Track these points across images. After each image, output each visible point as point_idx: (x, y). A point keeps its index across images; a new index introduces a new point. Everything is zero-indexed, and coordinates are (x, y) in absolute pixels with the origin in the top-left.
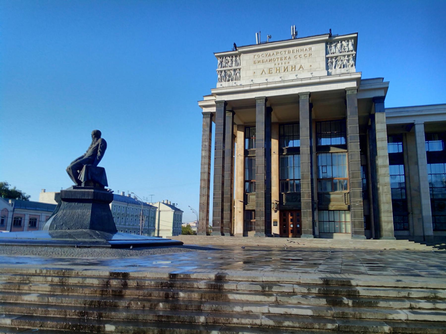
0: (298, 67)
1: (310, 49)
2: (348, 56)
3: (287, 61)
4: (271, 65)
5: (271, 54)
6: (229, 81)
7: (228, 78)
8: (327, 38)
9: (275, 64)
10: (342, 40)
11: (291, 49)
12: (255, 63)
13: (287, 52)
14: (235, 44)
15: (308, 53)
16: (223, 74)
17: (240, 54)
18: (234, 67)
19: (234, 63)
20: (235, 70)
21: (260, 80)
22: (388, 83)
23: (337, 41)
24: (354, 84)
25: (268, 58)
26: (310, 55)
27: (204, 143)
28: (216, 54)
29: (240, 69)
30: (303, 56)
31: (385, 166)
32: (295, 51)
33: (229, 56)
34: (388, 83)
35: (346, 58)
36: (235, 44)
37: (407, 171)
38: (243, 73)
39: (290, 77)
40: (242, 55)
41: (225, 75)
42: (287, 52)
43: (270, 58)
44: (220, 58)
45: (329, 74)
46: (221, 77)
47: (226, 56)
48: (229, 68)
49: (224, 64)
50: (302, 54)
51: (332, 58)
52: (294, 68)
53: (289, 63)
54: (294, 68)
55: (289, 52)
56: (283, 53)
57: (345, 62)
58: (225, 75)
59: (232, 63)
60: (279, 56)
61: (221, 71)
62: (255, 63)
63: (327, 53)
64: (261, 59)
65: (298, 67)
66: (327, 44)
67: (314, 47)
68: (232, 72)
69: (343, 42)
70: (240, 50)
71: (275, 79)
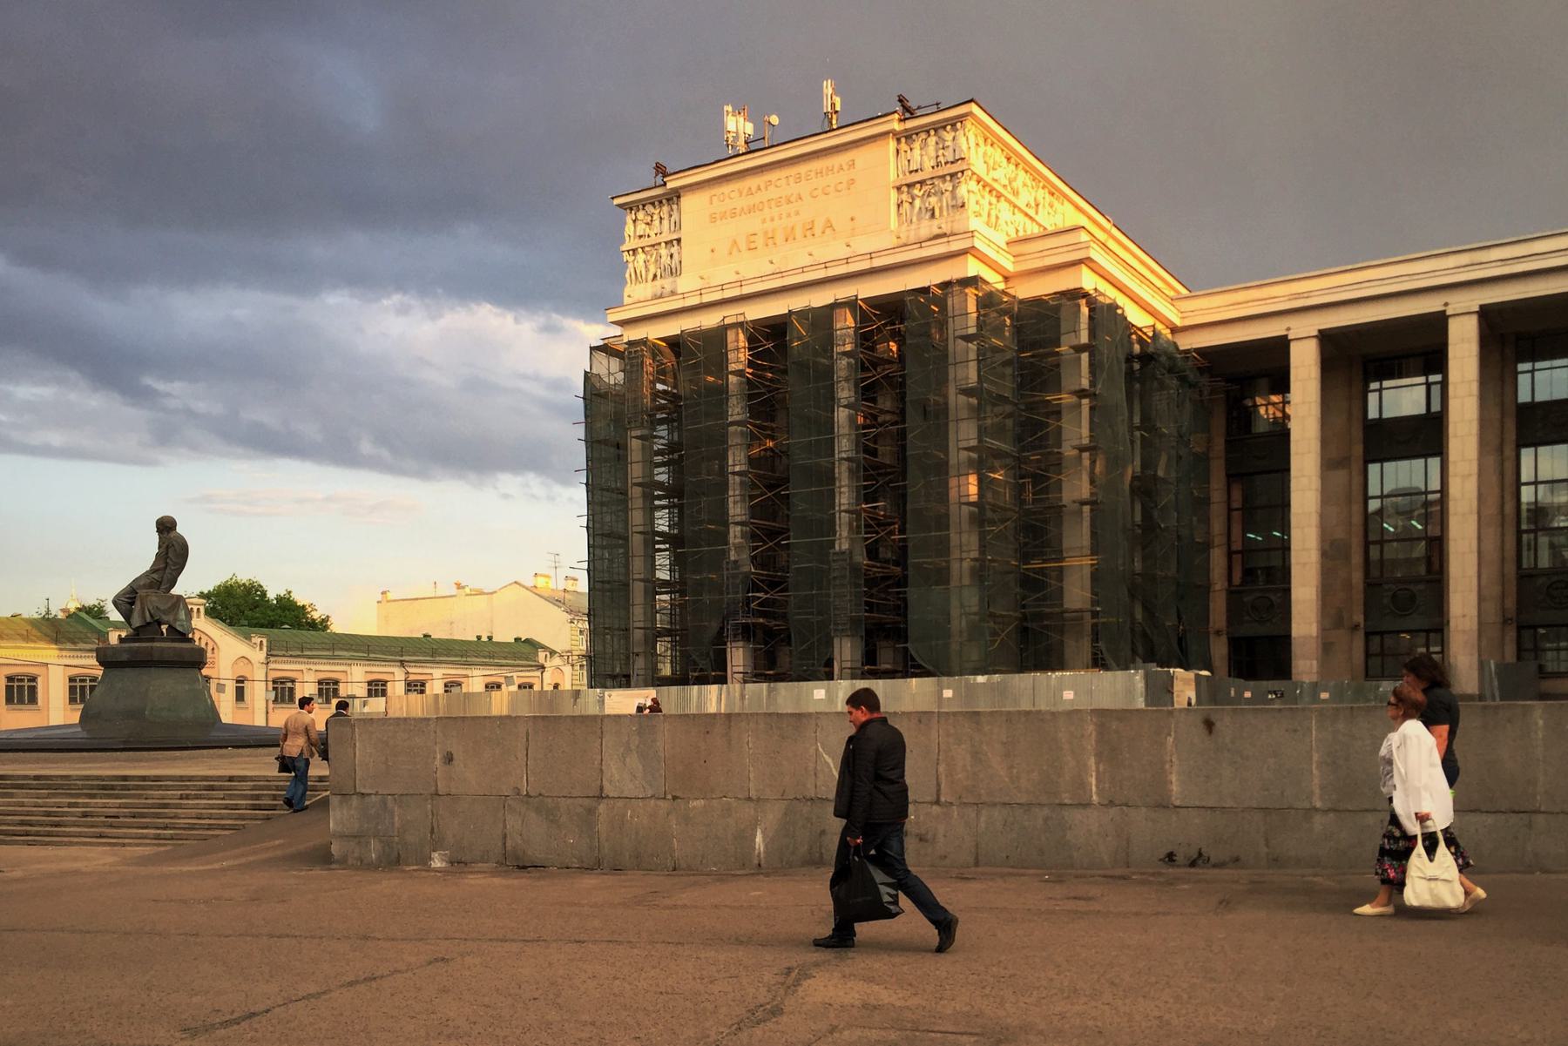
1: (852, 164)
9: (764, 221)
11: (802, 169)
12: (713, 219)
15: (844, 177)
18: (666, 237)
28: (616, 201)
29: (679, 240)
30: (831, 189)
37: (1509, 466)
38: (688, 253)
53: (797, 213)
56: (783, 182)
60: (773, 193)
62: (713, 219)
67: (861, 156)
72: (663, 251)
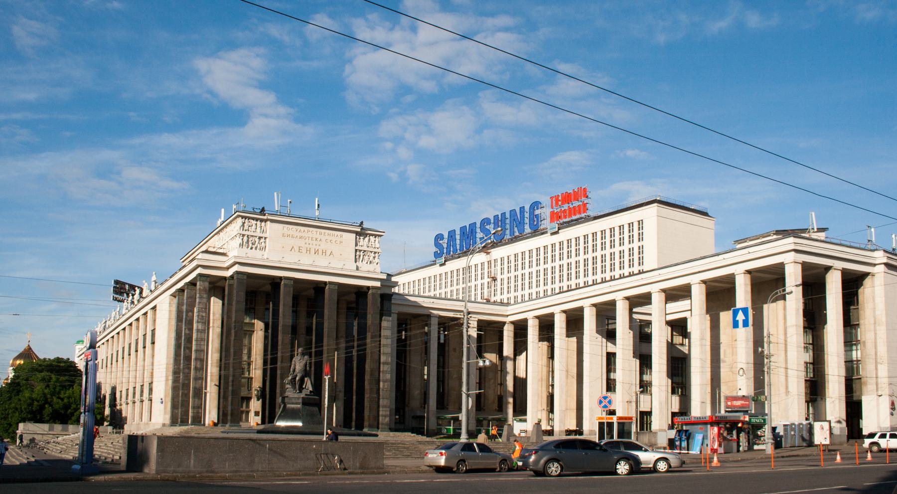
0: (328, 253)
1: (341, 236)
2: (375, 253)
3: (318, 243)
4: (301, 243)
7: (250, 245)
10: (372, 235)
15: (339, 239)
16: (245, 238)
17: (266, 221)
18: (258, 234)
19: (259, 229)
20: (260, 238)
23: (366, 235)
24: (378, 284)
25: (299, 234)
26: (341, 242)
31: (384, 363)
33: (253, 219)
35: (372, 255)
39: (322, 263)
40: (268, 223)
41: (248, 241)
43: (300, 234)
45: (357, 269)
47: (249, 218)
48: (252, 234)
49: (246, 227)
50: (334, 239)
51: (360, 251)
52: (324, 253)
54: (324, 253)
55: (321, 234)
57: (371, 258)
58: (248, 241)
60: (310, 234)
61: (243, 235)
63: (356, 245)
64: (290, 232)
65: (328, 253)
68: (257, 240)
71: (306, 261)
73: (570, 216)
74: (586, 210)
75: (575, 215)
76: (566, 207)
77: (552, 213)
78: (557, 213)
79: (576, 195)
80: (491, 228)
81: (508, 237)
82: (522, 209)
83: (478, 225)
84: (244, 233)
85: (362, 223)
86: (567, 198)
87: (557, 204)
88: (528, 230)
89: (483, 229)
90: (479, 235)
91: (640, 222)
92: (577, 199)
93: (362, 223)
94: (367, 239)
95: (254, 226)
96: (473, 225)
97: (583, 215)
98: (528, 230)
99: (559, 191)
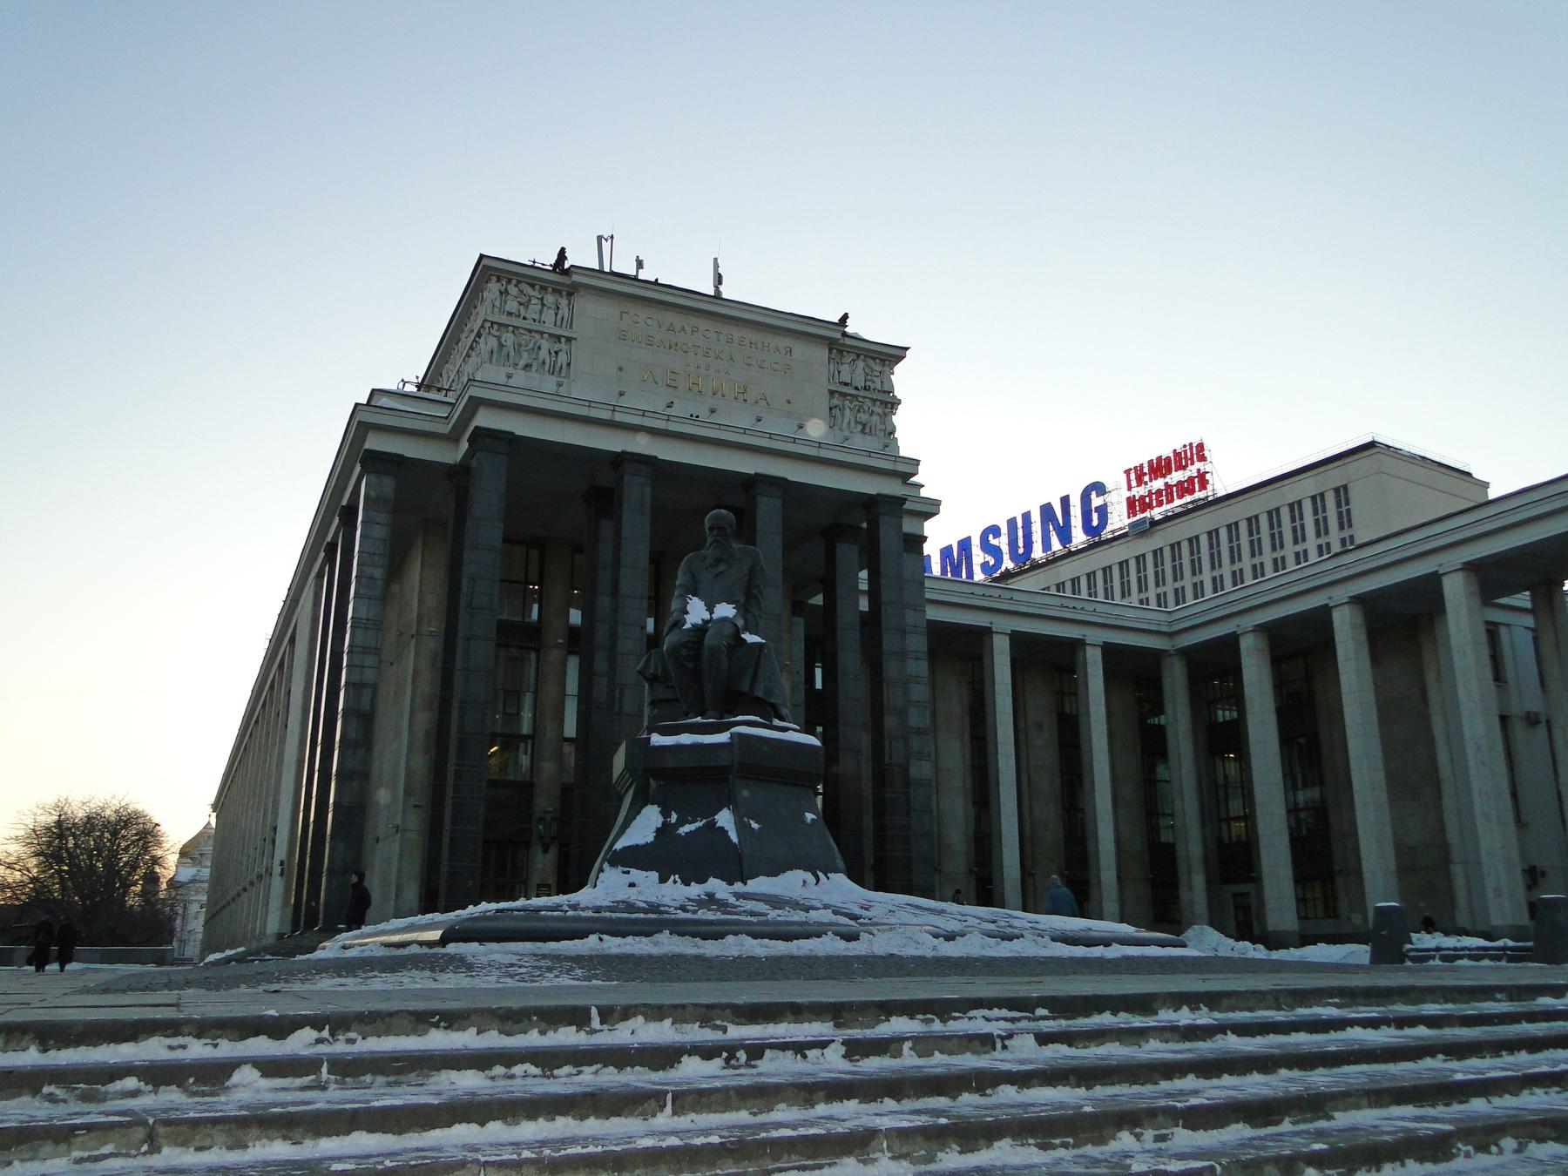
5: (677, 326)
6: (528, 367)
8: (838, 336)
12: (623, 336)
13: (722, 338)
14: (563, 251)
18: (549, 327)
21: (644, 401)
22: (936, 504)
27: (368, 570)
32: (747, 342)
34: (936, 504)
36: (562, 255)
42: (722, 338)
44: (499, 280)
46: (501, 346)
48: (528, 324)
55: (729, 341)
59: (541, 312)
62: (623, 336)
66: (830, 350)
69: (871, 362)
70: (575, 278)
72: (546, 345)
73: (1170, 500)
74: (1204, 484)
75: (1181, 497)
76: (1159, 484)
77: (1131, 503)
78: (1142, 498)
79: (1181, 459)
80: (1003, 542)
81: (1038, 553)
82: (1065, 501)
83: (976, 542)
84: (504, 319)
85: (845, 317)
86: (1160, 467)
87: (1140, 482)
88: (1079, 537)
89: (986, 547)
90: (978, 557)
91: (1342, 493)
92: (1180, 467)
93: (845, 317)
94: (861, 364)
95: (535, 306)
96: (965, 545)
97: (1198, 495)
98: (1079, 537)
99: (1143, 457)
